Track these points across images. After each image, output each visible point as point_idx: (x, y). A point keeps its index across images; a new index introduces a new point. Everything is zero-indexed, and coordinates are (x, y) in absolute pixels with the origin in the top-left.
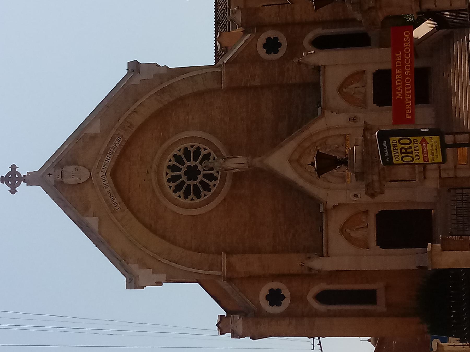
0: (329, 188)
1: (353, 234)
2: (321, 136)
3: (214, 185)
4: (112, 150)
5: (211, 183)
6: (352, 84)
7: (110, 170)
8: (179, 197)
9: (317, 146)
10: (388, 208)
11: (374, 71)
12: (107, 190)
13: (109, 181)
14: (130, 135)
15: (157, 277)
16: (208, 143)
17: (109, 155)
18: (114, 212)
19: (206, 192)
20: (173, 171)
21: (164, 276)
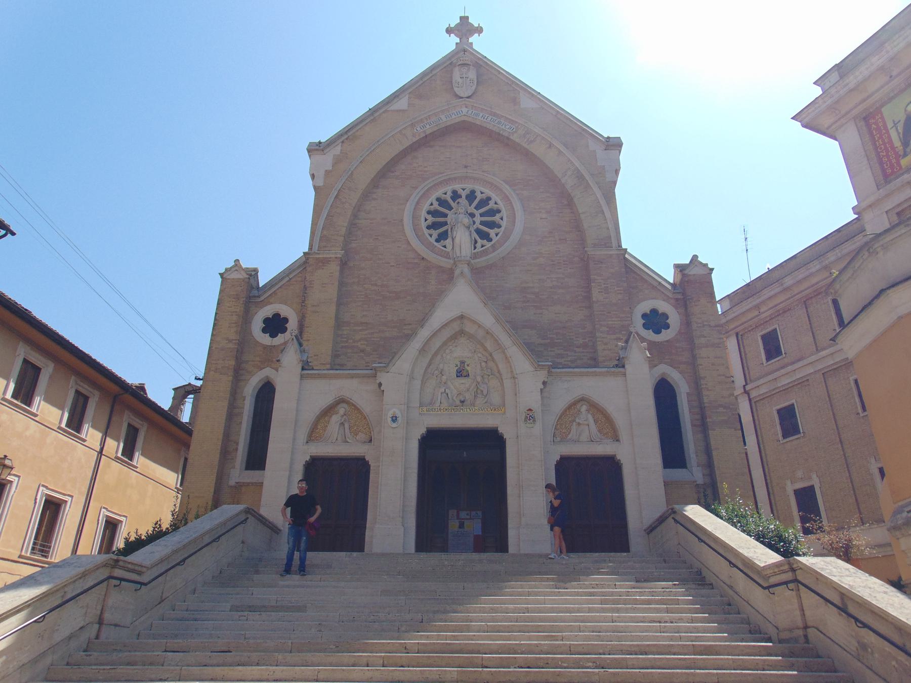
0: (412, 378)
1: (335, 419)
2: (501, 366)
4: (497, 121)
6: (596, 421)
7: (470, 120)
9: (486, 362)
10: (372, 476)
11: (618, 457)
13: (454, 118)
14: (517, 140)
15: (320, 174)
16: (506, 237)
17: (490, 118)
18: (413, 125)
20: (467, 197)
21: (320, 183)
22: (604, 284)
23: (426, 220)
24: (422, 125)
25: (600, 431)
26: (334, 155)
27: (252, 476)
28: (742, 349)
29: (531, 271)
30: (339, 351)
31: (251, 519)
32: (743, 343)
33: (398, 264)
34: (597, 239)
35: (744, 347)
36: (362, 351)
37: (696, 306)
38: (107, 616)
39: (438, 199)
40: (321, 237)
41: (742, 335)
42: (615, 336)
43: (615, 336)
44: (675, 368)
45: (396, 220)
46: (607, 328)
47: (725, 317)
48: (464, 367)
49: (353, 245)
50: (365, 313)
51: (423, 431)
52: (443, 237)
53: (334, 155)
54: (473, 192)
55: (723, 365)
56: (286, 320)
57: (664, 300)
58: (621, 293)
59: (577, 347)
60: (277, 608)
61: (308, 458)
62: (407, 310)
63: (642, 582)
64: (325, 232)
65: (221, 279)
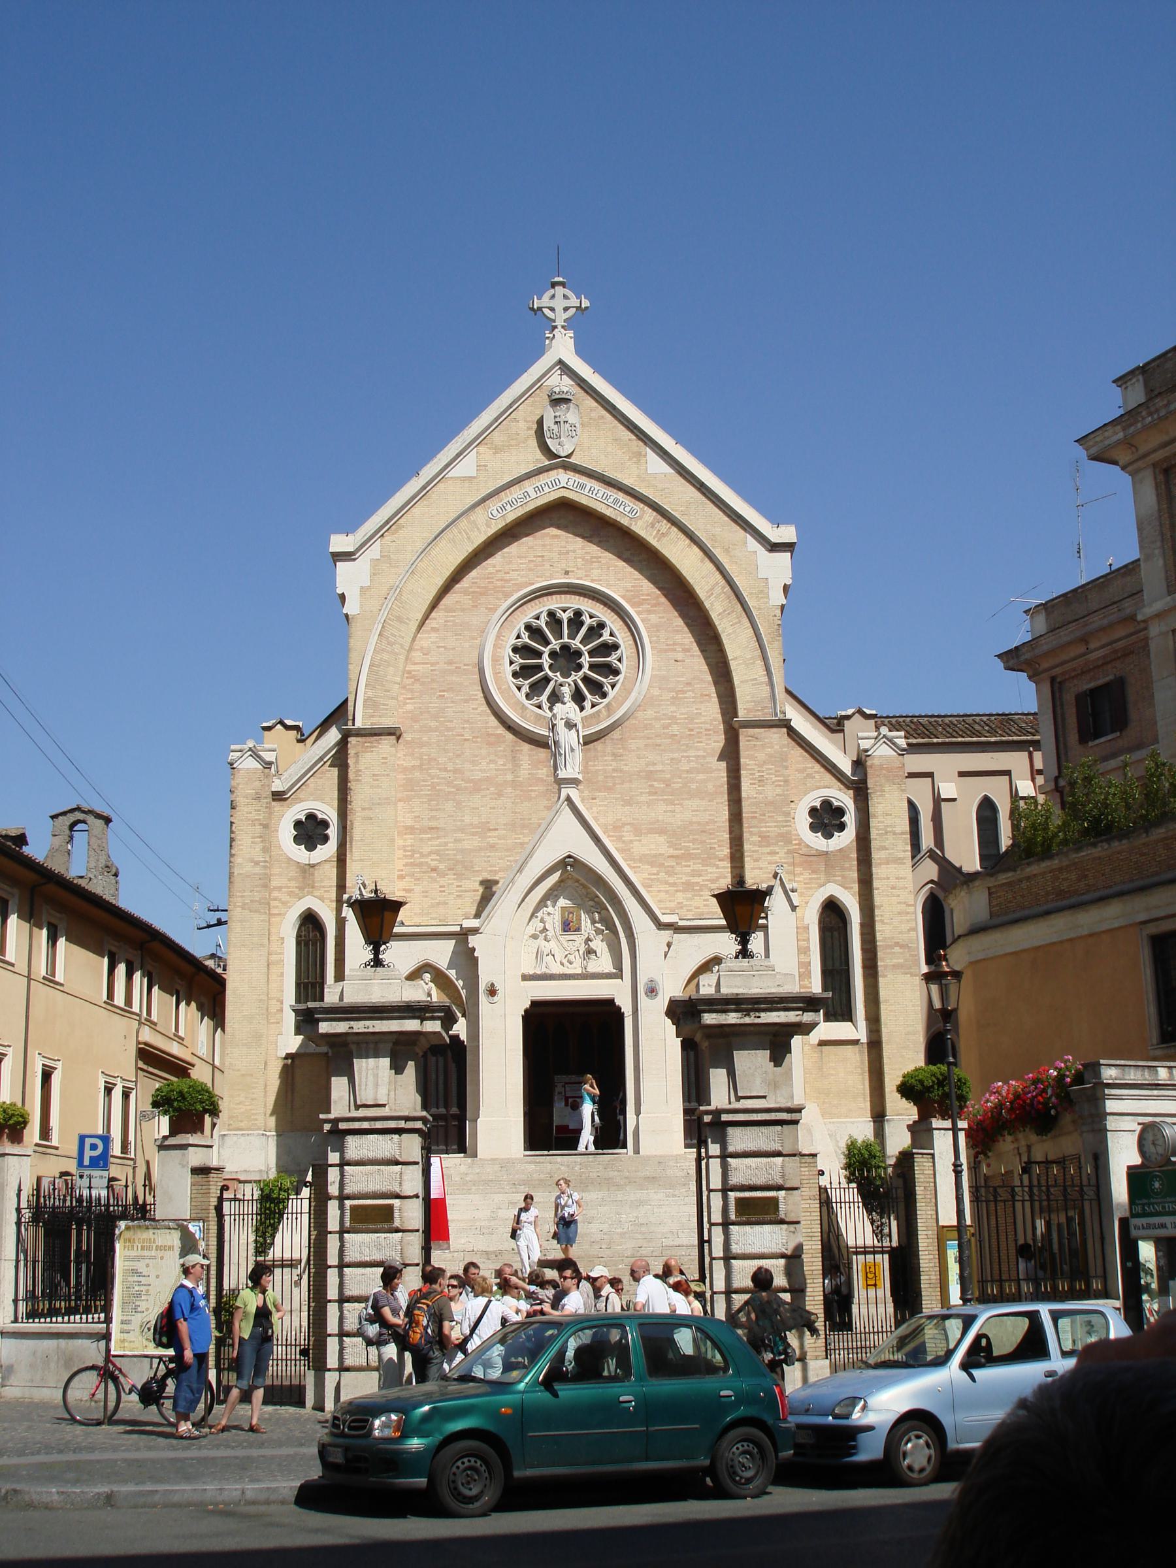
3: (539, 707)
5: (544, 698)
8: (515, 632)
17: (600, 495)
19: (525, 689)
22: (759, 771)
23: (511, 663)
24: (500, 505)
28: (1058, 708)
29: (660, 745)
32: (1061, 698)
35: (1062, 705)
36: (434, 870)
39: (528, 627)
40: (365, 701)
41: (1060, 683)
43: (768, 850)
44: (846, 888)
47: (1033, 649)
50: (434, 813)
51: (527, 1005)
52: (536, 689)
58: (780, 786)
64: (370, 693)
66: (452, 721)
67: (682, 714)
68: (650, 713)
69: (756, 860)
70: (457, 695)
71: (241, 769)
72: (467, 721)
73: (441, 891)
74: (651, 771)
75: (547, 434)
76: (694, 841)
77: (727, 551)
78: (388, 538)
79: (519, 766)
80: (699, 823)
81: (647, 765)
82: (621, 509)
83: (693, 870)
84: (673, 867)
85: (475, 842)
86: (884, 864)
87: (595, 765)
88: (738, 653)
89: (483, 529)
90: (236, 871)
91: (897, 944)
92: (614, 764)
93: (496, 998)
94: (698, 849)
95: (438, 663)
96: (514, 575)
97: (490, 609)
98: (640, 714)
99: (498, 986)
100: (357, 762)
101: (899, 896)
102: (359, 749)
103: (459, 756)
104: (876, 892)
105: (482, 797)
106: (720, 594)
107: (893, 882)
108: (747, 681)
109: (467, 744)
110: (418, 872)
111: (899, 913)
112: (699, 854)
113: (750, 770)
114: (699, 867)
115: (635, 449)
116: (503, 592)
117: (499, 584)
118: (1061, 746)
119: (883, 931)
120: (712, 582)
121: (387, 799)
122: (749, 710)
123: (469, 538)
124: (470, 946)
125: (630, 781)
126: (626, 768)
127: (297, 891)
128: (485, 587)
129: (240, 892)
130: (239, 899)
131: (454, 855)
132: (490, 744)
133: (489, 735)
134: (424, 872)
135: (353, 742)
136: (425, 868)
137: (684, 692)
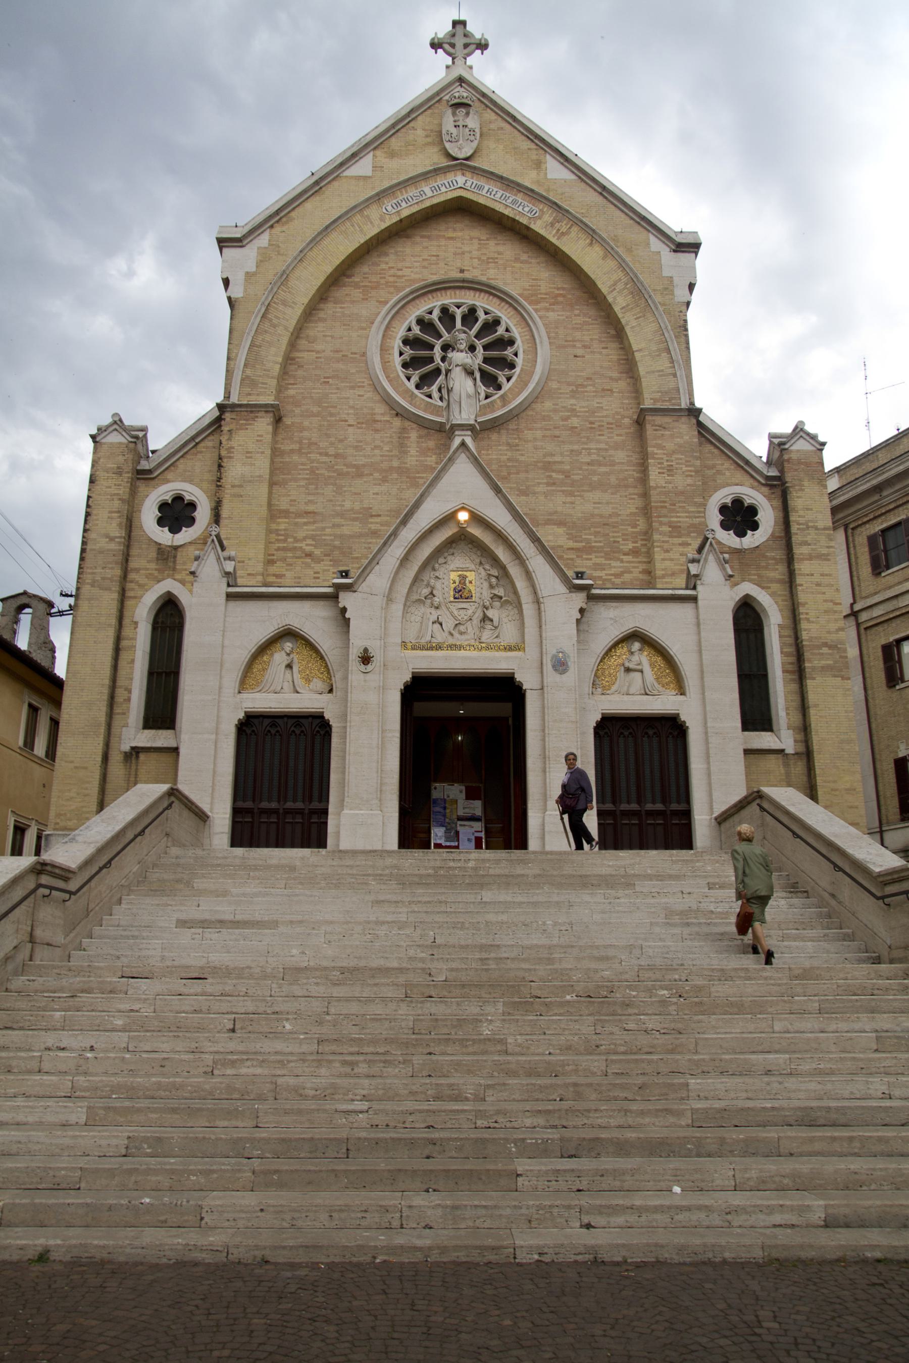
0: (389, 599)
3: (430, 396)
4: (511, 199)
5: (434, 388)
6: (652, 665)
9: (497, 577)
12: (427, 190)
14: (542, 232)
17: (499, 195)
19: (415, 379)
20: (464, 318)
23: (401, 354)
24: (395, 201)
25: (657, 679)
26: (259, 248)
27: (161, 738)
28: (852, 549)
29: (558, 437)
30: (273, 555)
31: (176, 804)
32: (854, 541)
33: (358, 423)
34: (658, 392)
35: (854, 547)
36: (309, 555)
37: (798, 497)
38: (38, 933)
40: (243, 380)
41: (853, 529)
42: (680, 540)
43: (680, 540)
44: (763, 588)
45: (355, 354)
46: (670, 527)
48: (465, 584)
49: (291, 392)
50: (311, 498)
51: (408, 677)
52: (425, 381)
53: (259, 248)
54: (472, 311)
55: (832, 585)
56: (192, 506)
57: (752, 488)
58: (691, 476)
59: (625, 554)
60: (236, 924)
61: (241, 715)
62: (374, 494)
63: (717, 889)
64: (249, 372)
65: (92, 444)
66: (335, 407)
67: (584, 407)
68: (548, 404)
69: (667, 551)
70: (342, 382)
71: (105, 444)
72: (352, 407)
73: (315, 578)
74: (549, 463)
75: (446, 137)
76: (596, 534)
77: (629, 250)
78: (278, 229)
79: (406, 453)
80: (601, 516)
81: (545, 456)
82: (520, 209)
83: (595, 564)
84: (572, 559)
85: (356, 528)
86: (807, 559)
87: (488, 455)
88: (643, 345)
89: (377, 222)
90: (89, 547)
91: (825, 645)
92: (509, 453)
93: (369, 667)
94: (600, 542)
95: (324, 351)
96: (406, 272)
97: (380, 302)
98: (538, 407)
99: (372, 652)
100: (229, 439)
101: (824, 593)
102: (233, 426)
103: (341, 441)
104: (800, 588)
105: (365, 482)
106: (624, 289)
107: (817, 578)
108: (653, 372)
109: (351, 430)
110: (292, 557)
111: (826, 612)
112: (601, 547)
113: (658, 459)
114: (603, 561)
115: (534, 157)
116: (395, 287)
117: (391, 279)
118: (855, 579)
119: (809, 630)
120: (615, 277)
121: (260, 476)
122: (655, 401)
123: (361, 230)
124: (341, 605)
125: (527, 472)
126: (522, 458)
127: (156, 573)
128: (377, 282)
129: (91, 568)
130: (89, 576)
131: (331, 540)
132: (376, 431)
133: (376, 421)
134: (297, 558)
135: (228, 419)
136: (299, 553)
137: (582, 386)
